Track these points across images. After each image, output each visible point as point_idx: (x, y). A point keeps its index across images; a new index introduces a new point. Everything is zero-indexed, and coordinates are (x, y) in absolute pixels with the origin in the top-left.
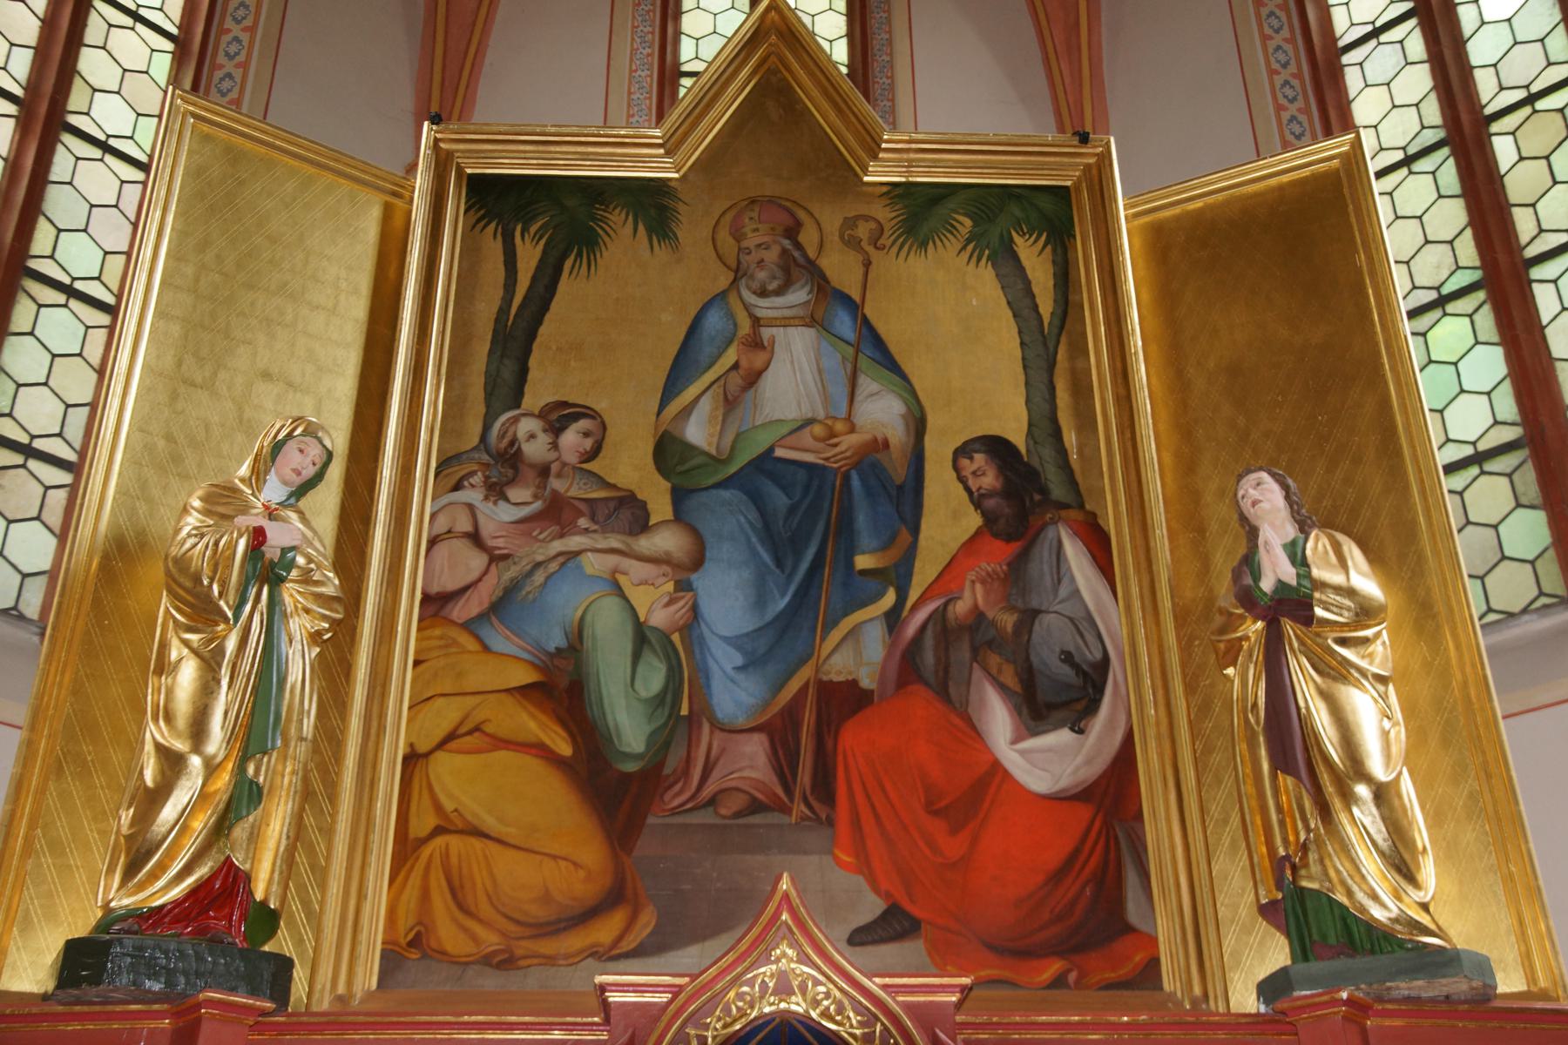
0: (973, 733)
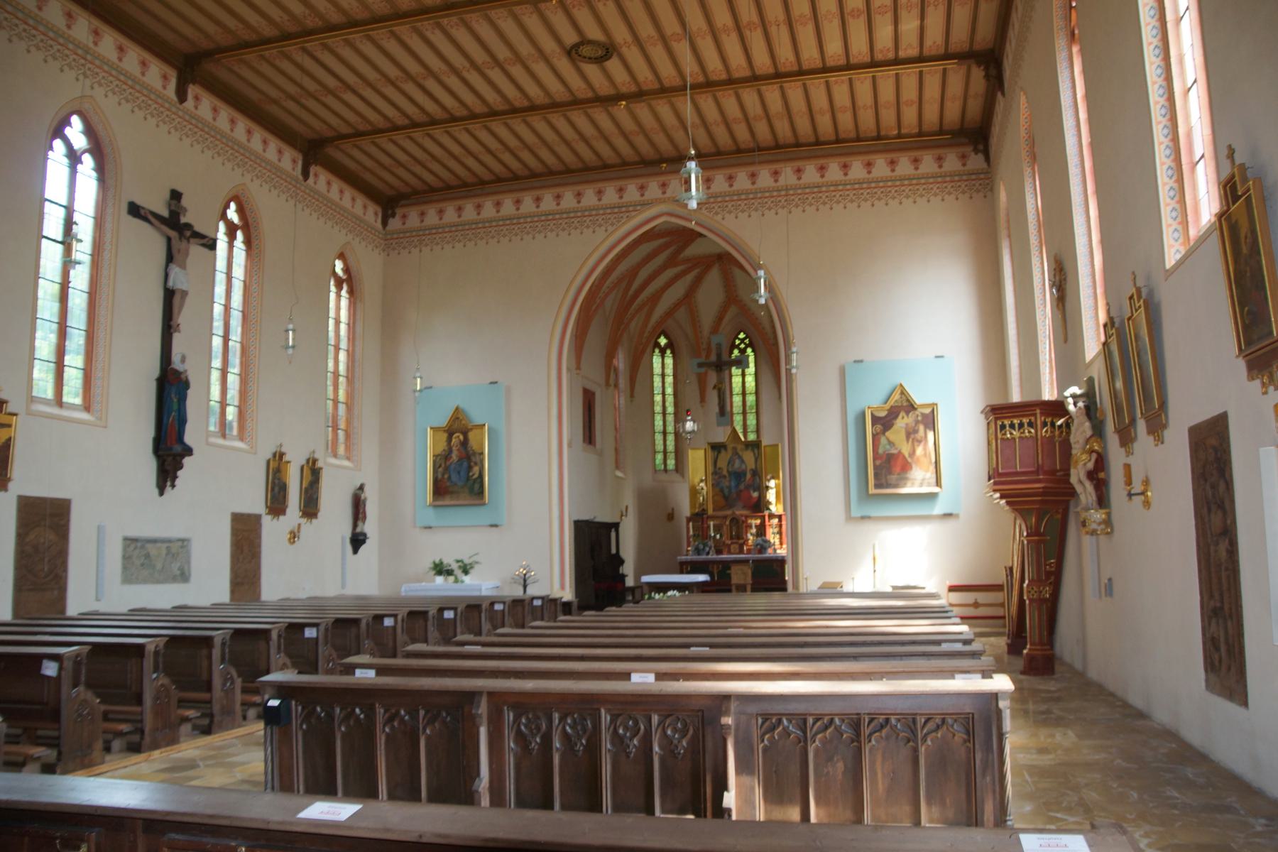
0: (750, 493)
